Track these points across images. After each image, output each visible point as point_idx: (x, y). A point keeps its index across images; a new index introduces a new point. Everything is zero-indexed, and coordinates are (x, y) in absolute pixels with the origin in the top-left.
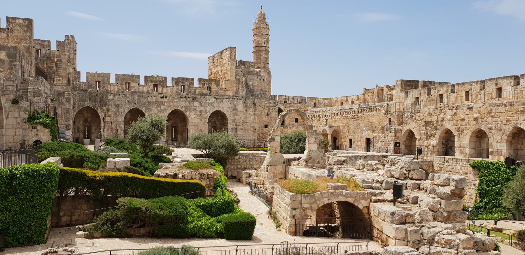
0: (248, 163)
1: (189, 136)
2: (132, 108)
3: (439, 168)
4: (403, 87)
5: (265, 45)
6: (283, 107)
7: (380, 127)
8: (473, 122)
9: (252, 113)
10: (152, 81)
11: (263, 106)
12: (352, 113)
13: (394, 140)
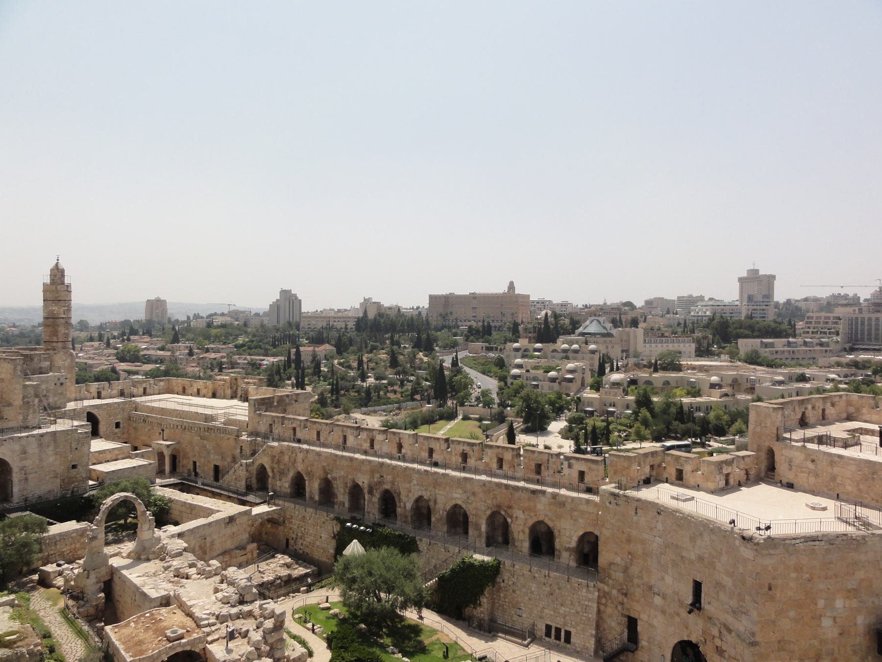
0: (53, 548)
3: (290, 517)
4: (257, 407)
5: (64, 316)
6: (96, 410)
7: (230, 453)
11: (68, 440)
12: (196, 429)
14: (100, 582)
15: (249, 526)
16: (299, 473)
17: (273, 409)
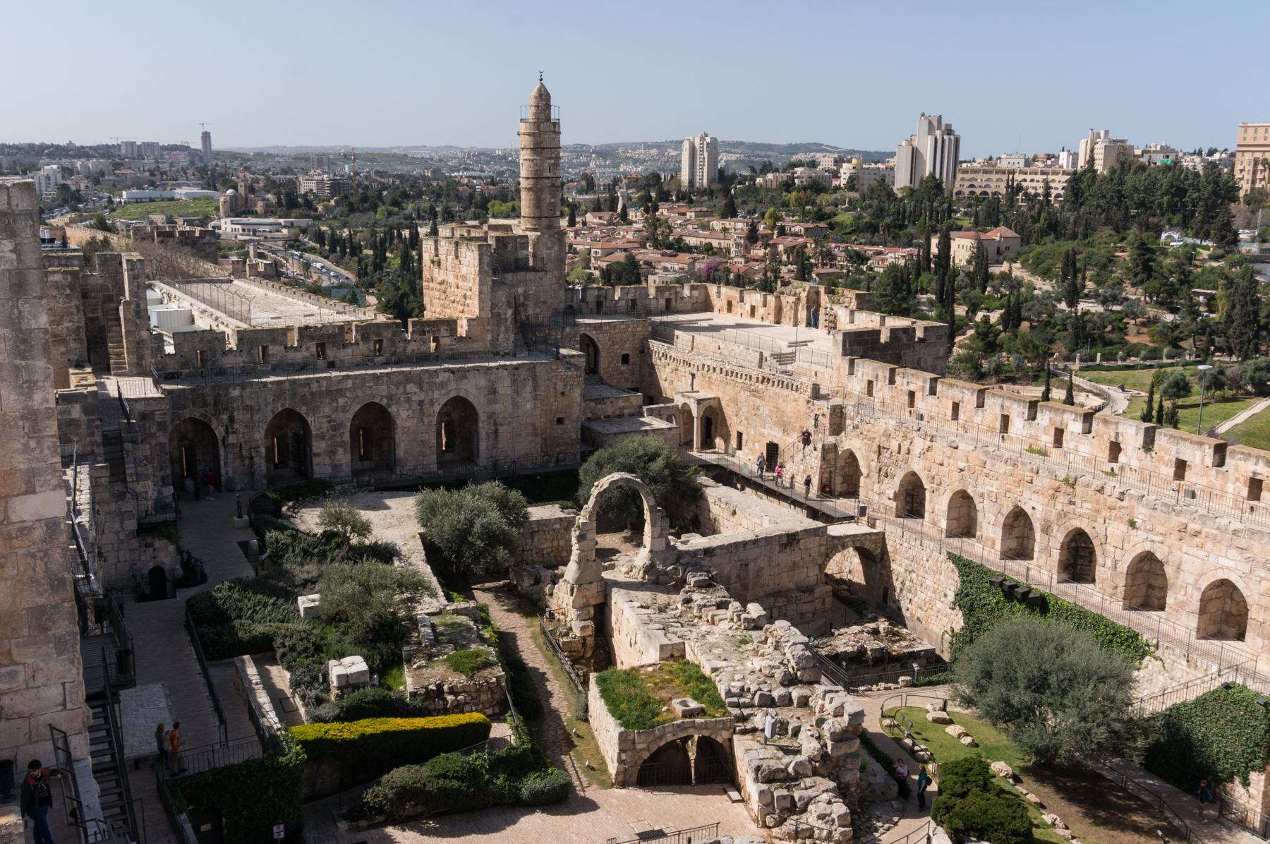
0: (529, 541)
1: (397, 457)
2: (280, 409)
5: (549, 175)
8: (956, 475)
9: (528, 396)
10: (312, 338)
13: (821, 468)
14: (589, 606)
15: (820, 554)
16: (914, 474)
17: (877, 353)
